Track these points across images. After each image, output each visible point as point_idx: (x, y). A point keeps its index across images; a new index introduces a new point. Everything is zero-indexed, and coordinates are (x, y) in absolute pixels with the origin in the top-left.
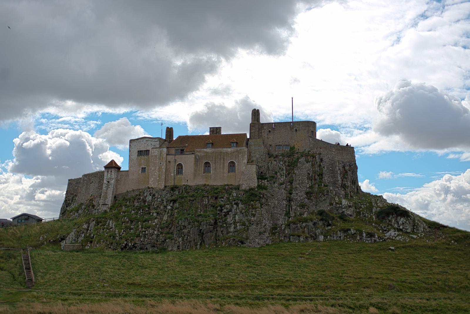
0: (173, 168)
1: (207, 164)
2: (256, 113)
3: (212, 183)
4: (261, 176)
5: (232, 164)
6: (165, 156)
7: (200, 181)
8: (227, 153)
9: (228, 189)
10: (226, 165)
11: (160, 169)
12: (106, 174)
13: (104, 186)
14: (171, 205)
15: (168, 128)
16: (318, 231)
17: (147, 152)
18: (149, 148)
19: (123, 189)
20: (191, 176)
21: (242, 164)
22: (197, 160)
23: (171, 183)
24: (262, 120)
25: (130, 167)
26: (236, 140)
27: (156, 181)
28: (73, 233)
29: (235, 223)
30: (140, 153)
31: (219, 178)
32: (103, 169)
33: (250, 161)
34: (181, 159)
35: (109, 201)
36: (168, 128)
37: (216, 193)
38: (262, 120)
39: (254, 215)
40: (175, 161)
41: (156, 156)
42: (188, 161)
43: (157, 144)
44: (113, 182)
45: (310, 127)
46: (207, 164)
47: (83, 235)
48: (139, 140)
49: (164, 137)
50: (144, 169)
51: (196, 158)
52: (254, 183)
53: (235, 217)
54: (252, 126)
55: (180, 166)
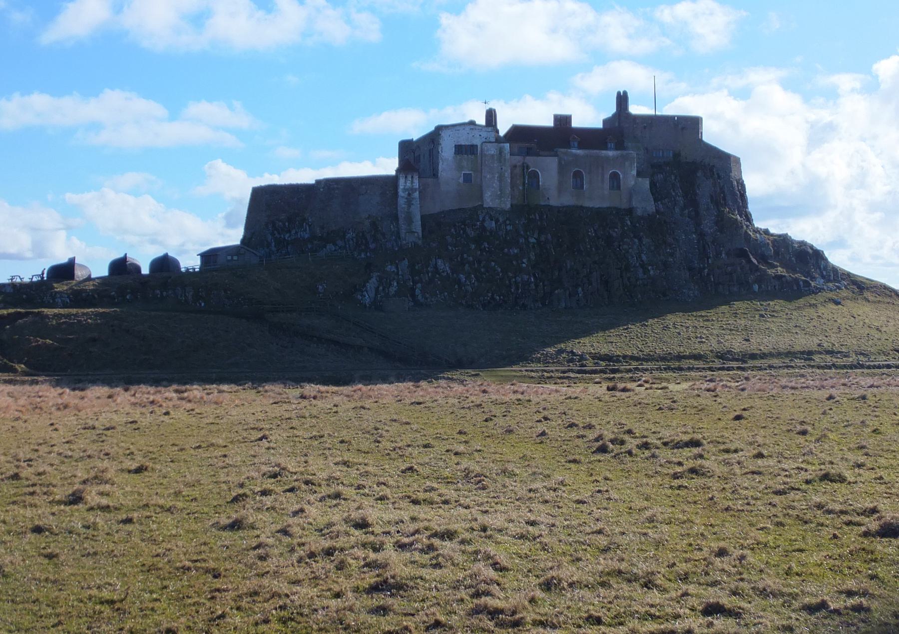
1: (578, 175)
2: (622, 100)
5: (615, 177)
7: (567, 200)
8: (607, 158)
10: (607, 176)
11: (501, 179)
12: (402, 181)
13: (402, 202)
14: (536, 236)
18: (477, 142)
19: (435, 208)
24: (635, 109)
26: (588, 137)
28: (374, 280)
31: (597, 196)
39: (672, 255)
41: (493, 156)
42: (548, 169)
44: (417, 194)
45: (692, 124)
46: (578, 175)
47: (395, 284)
48: (458, 128)
51: (560, 163)
53: (640, 257)
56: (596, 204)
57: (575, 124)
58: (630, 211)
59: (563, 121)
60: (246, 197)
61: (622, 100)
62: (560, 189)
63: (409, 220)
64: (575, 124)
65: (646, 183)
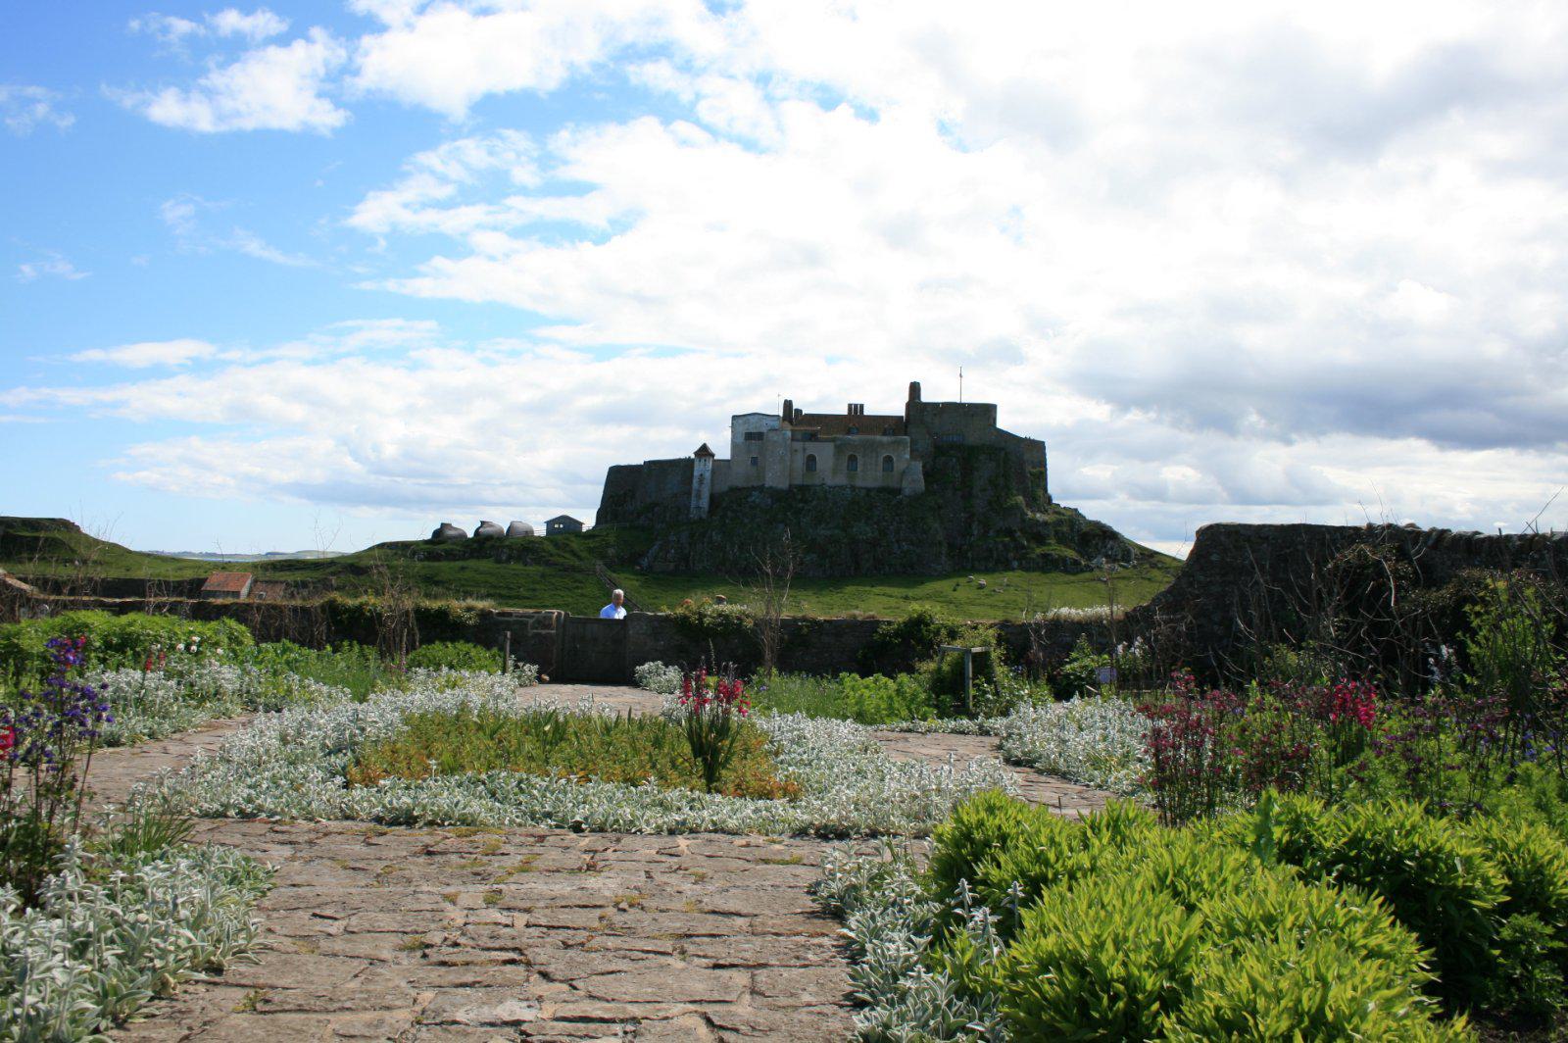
0: (800, 462)
2: (915, 389)
3: (859, 483)
4: (927, 475)
5: (889, 460)
6: (789, 442)
7: (841, 480)
8: (881, 444)
10: (881, 459)
12: (696, 463)
13: (695, 481)
15: (786, 401)
16: (1011, 555)
17: (759, 436)
18: (764, 430)
21: (903, 458)
22: (839, 449)
23: (798, 482)
24: (926, 397)
25: (733, 455)
27: (776, 477)
29: (897, 541)
30: (749, 436)
31: (870, 476)
32: (693, 456)
33: (913, 457)
34: (812, 448)
35: (705, 503)
36: (786, 401)
38: (926, 397)
40: (804, 450)
44: (708, 475)
45: (988, 411)
46: (853, 459)
49: (781, 414)
50: (754, 461)
52: (921, 485)
54: (908, 405)
56: (870, 484)
58: (899, 491)
59: (856, 410)
60: (602, 476)
61: (915, 389)
62: (835, 471)
63: (699, 497)
65: (919, 466)
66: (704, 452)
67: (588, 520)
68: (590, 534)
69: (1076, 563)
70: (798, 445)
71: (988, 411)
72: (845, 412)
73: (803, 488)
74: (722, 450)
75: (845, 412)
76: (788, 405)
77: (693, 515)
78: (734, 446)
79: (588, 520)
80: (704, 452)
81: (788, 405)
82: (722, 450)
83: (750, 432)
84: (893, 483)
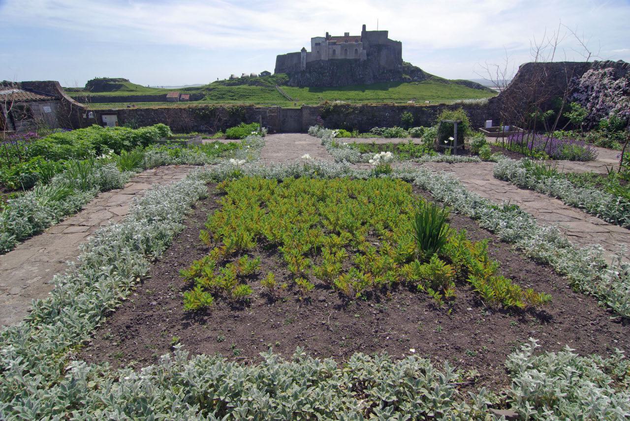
0: (331, 51)
2: (364, 27)
3: (348, 58)
4: (368, 55)
5: (356, 50)
7: (343, 57)
9: (356, 60)
19: (310, 60)
20: (339, 55)
21: (361, 50)
24: (368, 29)
27: (324, 57)
30: (316, 44)
31: (351, 56)
33: (364, 49)
34: (334, 47)
35: (305, 66)
37: (349, 61)
38: (368, 29)
43: (324, 40)
45: (386, 33)
46: (346, 50)
50: (318, 52)
52: (365, 58)
55: (334, 51)
57: (350, 35)
59: (347, 34)
61: (364, 27)
62: (341, 54)
63: (303, 64)
64: (350, 35)
65: (365, 51)
66: (303, 50)
67: (272, 73)
68: (273, 76)
69: (409, 79)
70: (330, 46)
71: (386, 33)
72: (343, 35)
73: (332, 60)
74: (309, 50)
75: (343, 35)
76: (327, 34)
77: (302, 69)
78: (312, 48)
79: (272, 73)
80: (303, 50)
81: (327, 34)
82: (309, 50)
83: (316, 42)
84: (357, 57)
